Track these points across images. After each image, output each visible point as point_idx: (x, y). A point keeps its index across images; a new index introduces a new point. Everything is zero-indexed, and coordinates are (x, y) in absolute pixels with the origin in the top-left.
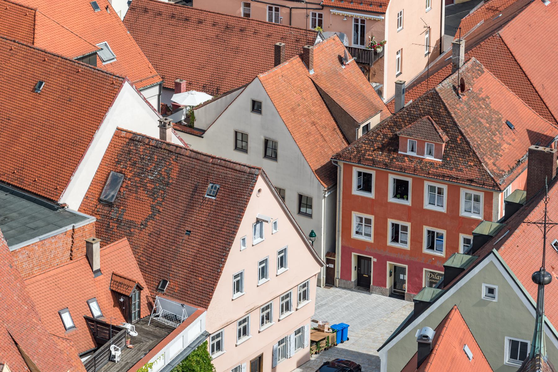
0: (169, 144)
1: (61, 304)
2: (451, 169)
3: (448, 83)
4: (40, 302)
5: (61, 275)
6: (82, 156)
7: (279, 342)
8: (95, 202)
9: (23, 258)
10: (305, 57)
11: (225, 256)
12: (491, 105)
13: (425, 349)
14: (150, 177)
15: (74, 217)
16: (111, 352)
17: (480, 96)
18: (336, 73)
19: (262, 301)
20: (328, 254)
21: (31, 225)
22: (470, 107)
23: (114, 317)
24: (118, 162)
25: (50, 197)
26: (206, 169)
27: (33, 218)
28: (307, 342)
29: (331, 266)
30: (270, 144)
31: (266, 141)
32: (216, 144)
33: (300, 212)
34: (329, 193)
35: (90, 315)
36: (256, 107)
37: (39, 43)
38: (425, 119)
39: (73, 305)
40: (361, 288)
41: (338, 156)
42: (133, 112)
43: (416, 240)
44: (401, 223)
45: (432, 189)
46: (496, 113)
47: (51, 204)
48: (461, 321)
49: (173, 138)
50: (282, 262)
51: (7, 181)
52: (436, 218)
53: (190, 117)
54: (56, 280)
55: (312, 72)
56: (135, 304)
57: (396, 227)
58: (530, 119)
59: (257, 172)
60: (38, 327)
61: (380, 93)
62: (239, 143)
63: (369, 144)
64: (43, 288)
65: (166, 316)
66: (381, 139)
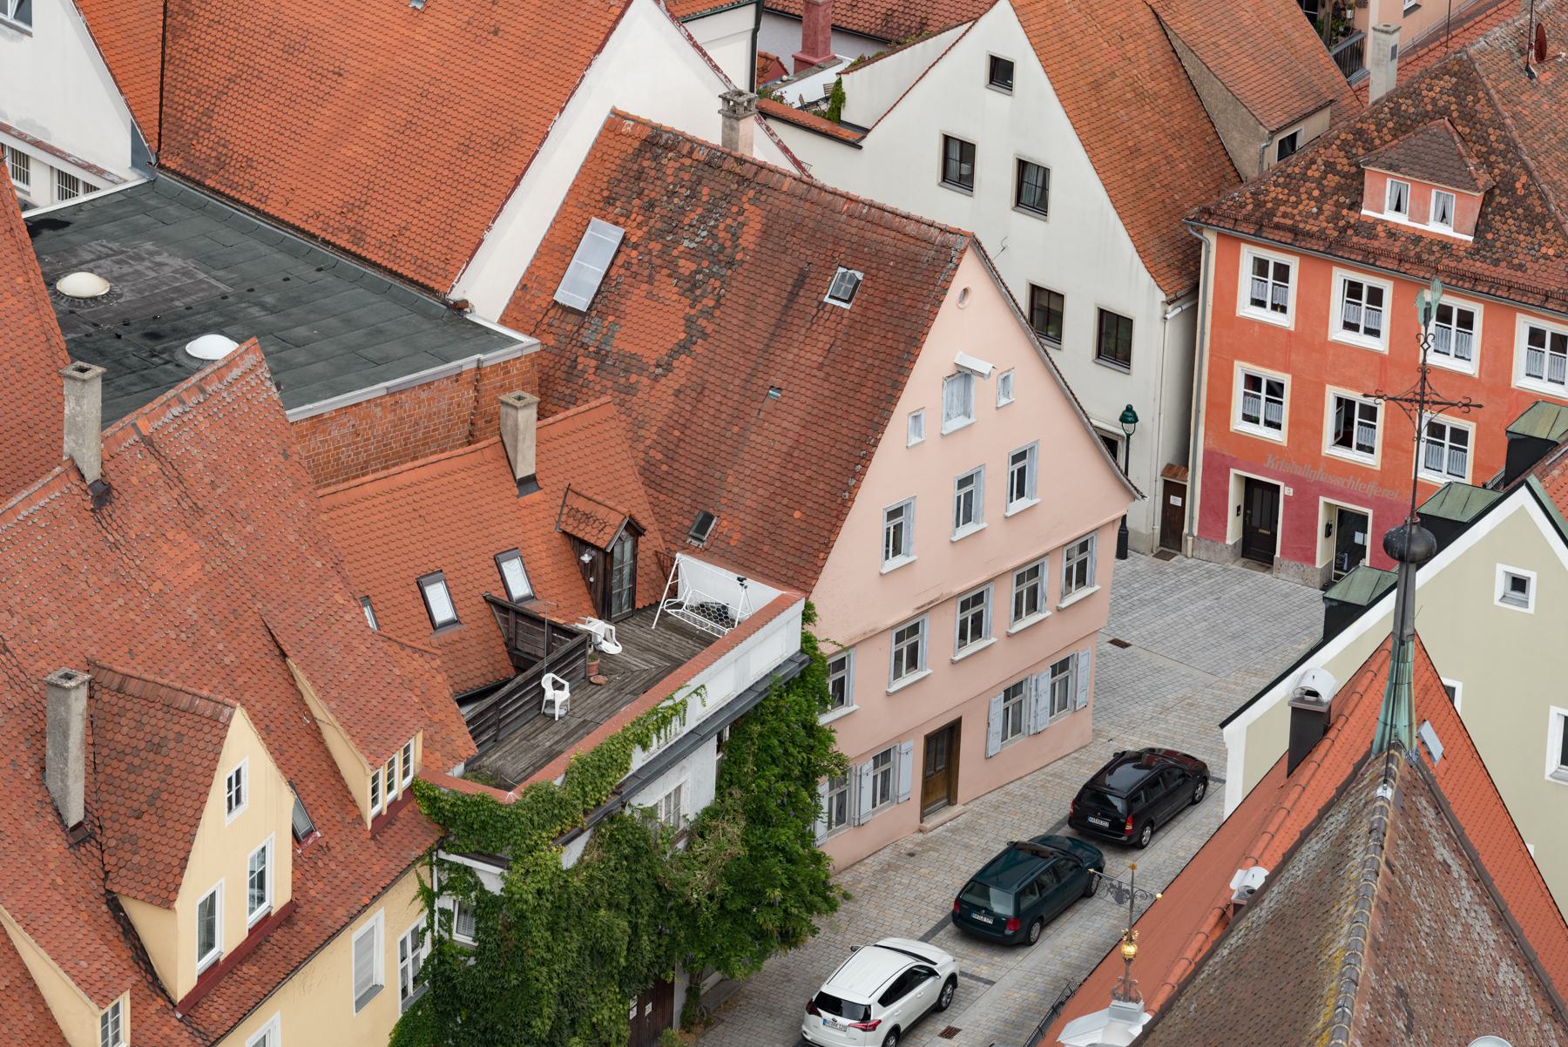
0: (741, 161)
1: (425, 560)
2: (1496, 263)
4: (371, 552)
5: (429, 485)
7: (1007, 692)
9: (343, 436)
11: (866, 459)
14: (686, 243)
15: (484, 338)
16: (543, 691)
20: (1168, 469)
21: (371, 352)
25: (427, 282)
27: (377, 333)
29: (1175, 501)
30: (1031, 177)
31: (1022, 165)
35: (499, 594)
39: (457, 566)
40: (1252, 563)
51: (323, 235)
54: (416, 497)
56: (621, 570)
57: (1345, 406)
59: (961, 243)
60: (348, 617)
62: (954, 165)
63: (1285, 186)
64: (379, 516)
65: (702, 609)
66: (1317, 174)
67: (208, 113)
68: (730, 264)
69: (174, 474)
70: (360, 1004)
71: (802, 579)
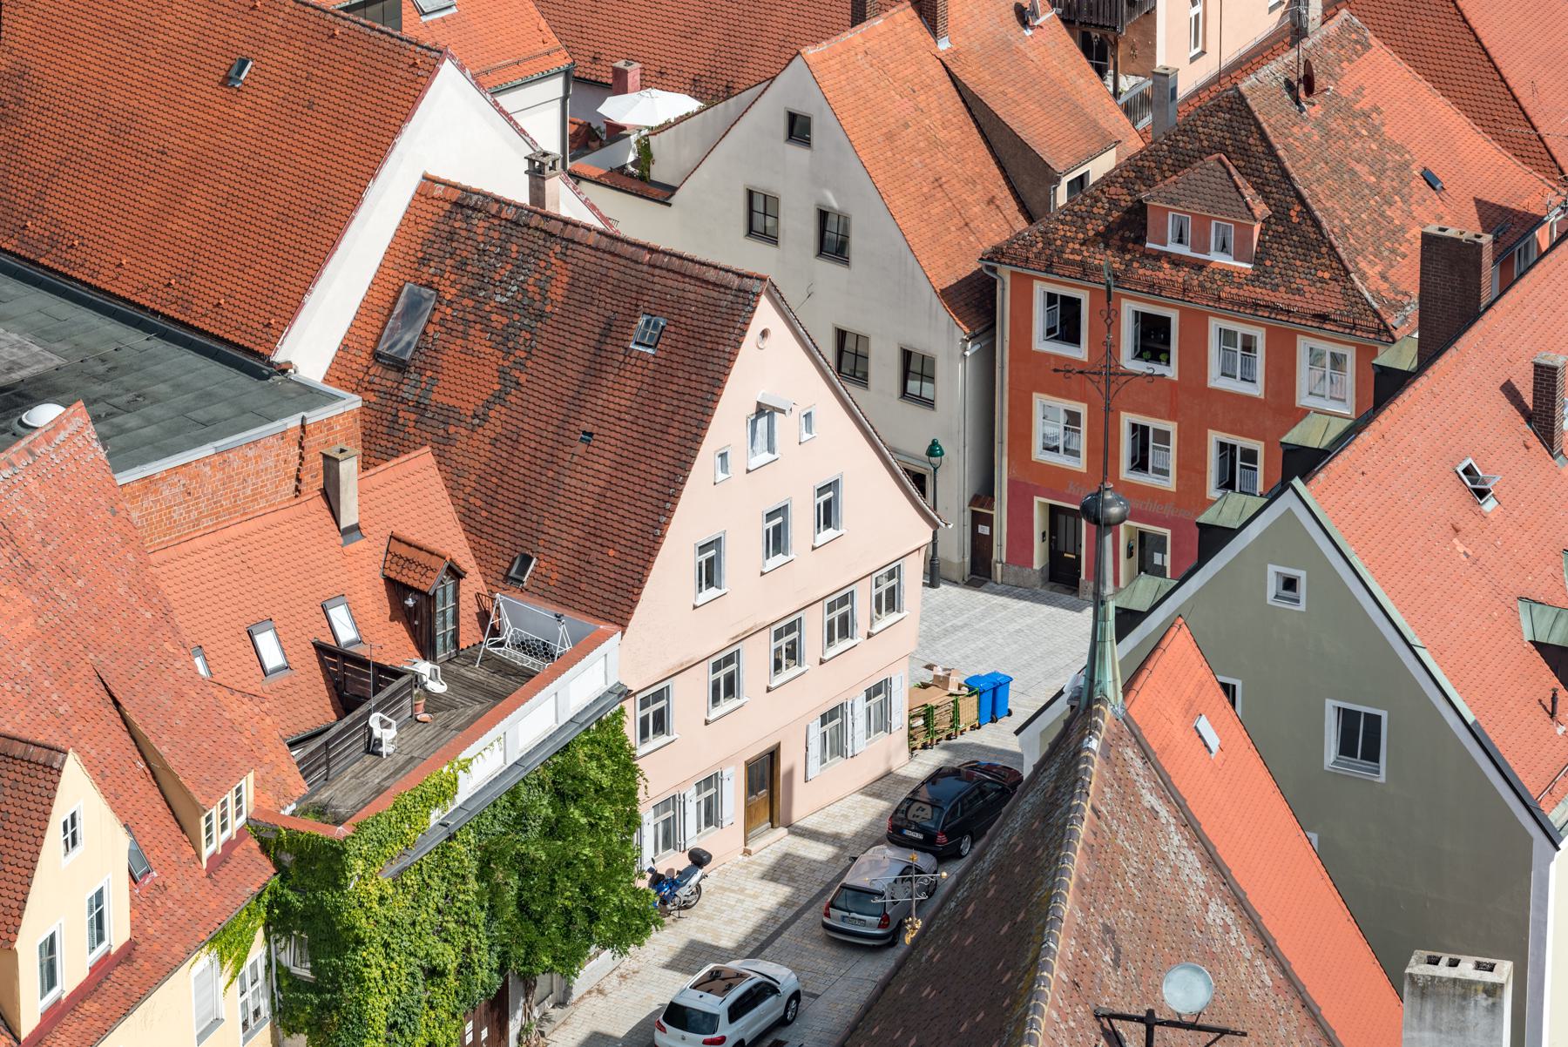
1: (254, 609)
4: (201, 604)
5: (256, 537)
6: (334, 245)
7: (823, 717)
8: (364, 358)
9: (174, 495)
11: (674, 498)
12: (1383, 129)
14: (498, 298)
15: (309, 396)
16: (370, 730)
17: (1357, 107)
18: (1007, 46)
19: (778, 611)
20: (975, 500)
21: (200, 414)
22: (1328, 134)
23: (391, 645)
24: (424, 261)
25: (251, 346)
27: (207, 397)
28: (899, 718)
29: (984, 530)
33: (904, 394)
34: (977, 347)
35: (328, 640)
36: (798, 129)
38: (1211, 161)
39: (286, 614)
40: (1059, 586)
41: (996, 255)
43: (1191, 466)
44: (1153, 423)
45: (1227, 337)
46: (1398, 149)
47: (254, 362)
48: (1194, 656)
50: (828, 515)
51: (152, 306)
52: (1236, 410)
54: (244, 549)
55: (944, 45)
56: (444, 612)
57: (1140, 432)
59: (756, 286)
60: (178, 665)
62: (758, 218)
63: (1073, 223)
64: (210, 569)
65: (523, 646)
67: (41, 195)
70: (201, 1037)
71: (619, 613)
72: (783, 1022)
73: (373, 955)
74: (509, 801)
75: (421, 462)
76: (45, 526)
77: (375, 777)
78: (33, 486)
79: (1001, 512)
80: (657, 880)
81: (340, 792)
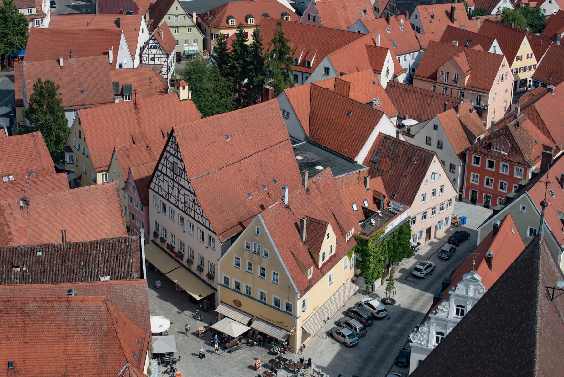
3: (512, 123)
6: (365, 143)
8: (369, 161)
10: (456, 109)
13: (496, 229)
15: (360, 167)
18: (468, 116)
19: (433, 205)
20: (460, 188)
22: (520, 133)
23: (374, 208)
24: (379, 146)
26: (413, 150)
27: (344, 166)
28: (449, 223)
31: (439, 142)
32: (418, 141)
33: (450, 171)
36: (436, 127)
37: (351, 96)
38: (502, 137)
41: (467, 149)
42: (386, 126)
43: (496, 185)
44: (490, 178)
45: (503, 165)
47: (352, 161)
48: (511, 219)
49: (402, 138)
50: (442, 190)
53: (409, 130)
55: (458, 115)
57: (488, 179)
58: (543, 140)
61: (485, 125)
65: (394, 209)
68: (398, 156)
69: (318, 187)
72: (432, 271)
73: (371, 257)
74: (392, 233)
75: (379, 179)
76: (324, 186)
77: (372, 229)
78: (322, 180)
79: (464, 191)
80: (412, 247)
81: (367, 231)
